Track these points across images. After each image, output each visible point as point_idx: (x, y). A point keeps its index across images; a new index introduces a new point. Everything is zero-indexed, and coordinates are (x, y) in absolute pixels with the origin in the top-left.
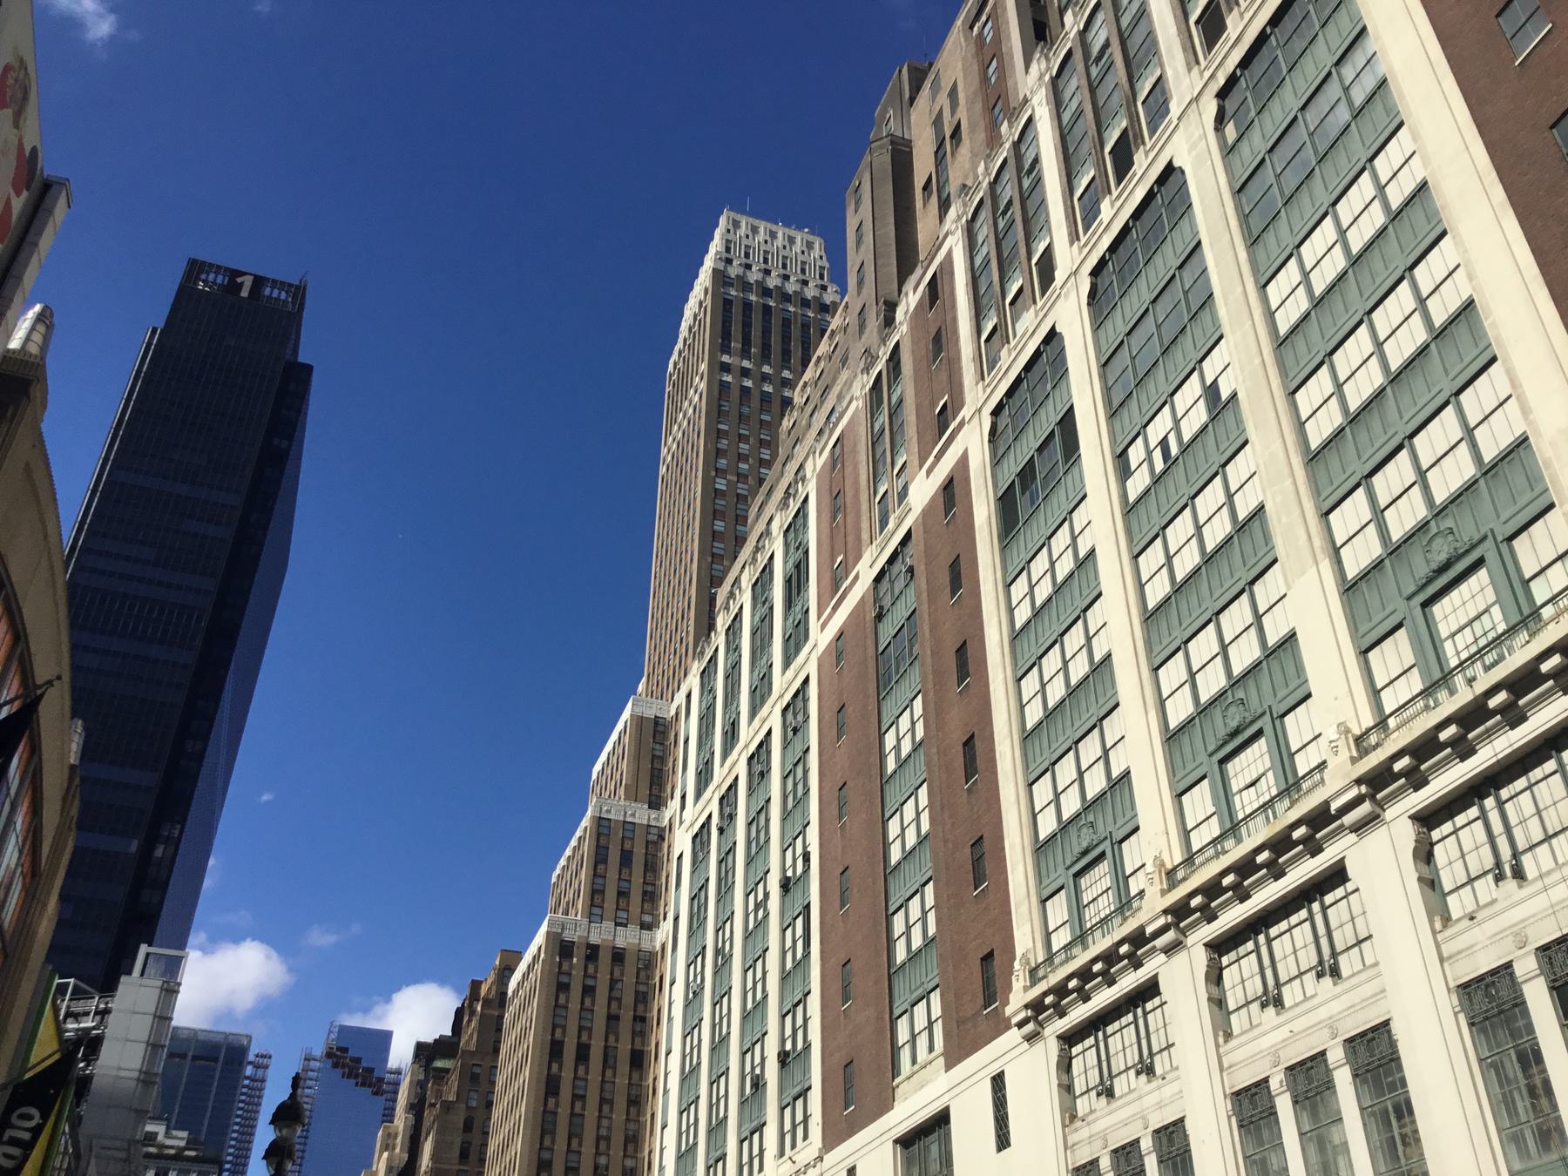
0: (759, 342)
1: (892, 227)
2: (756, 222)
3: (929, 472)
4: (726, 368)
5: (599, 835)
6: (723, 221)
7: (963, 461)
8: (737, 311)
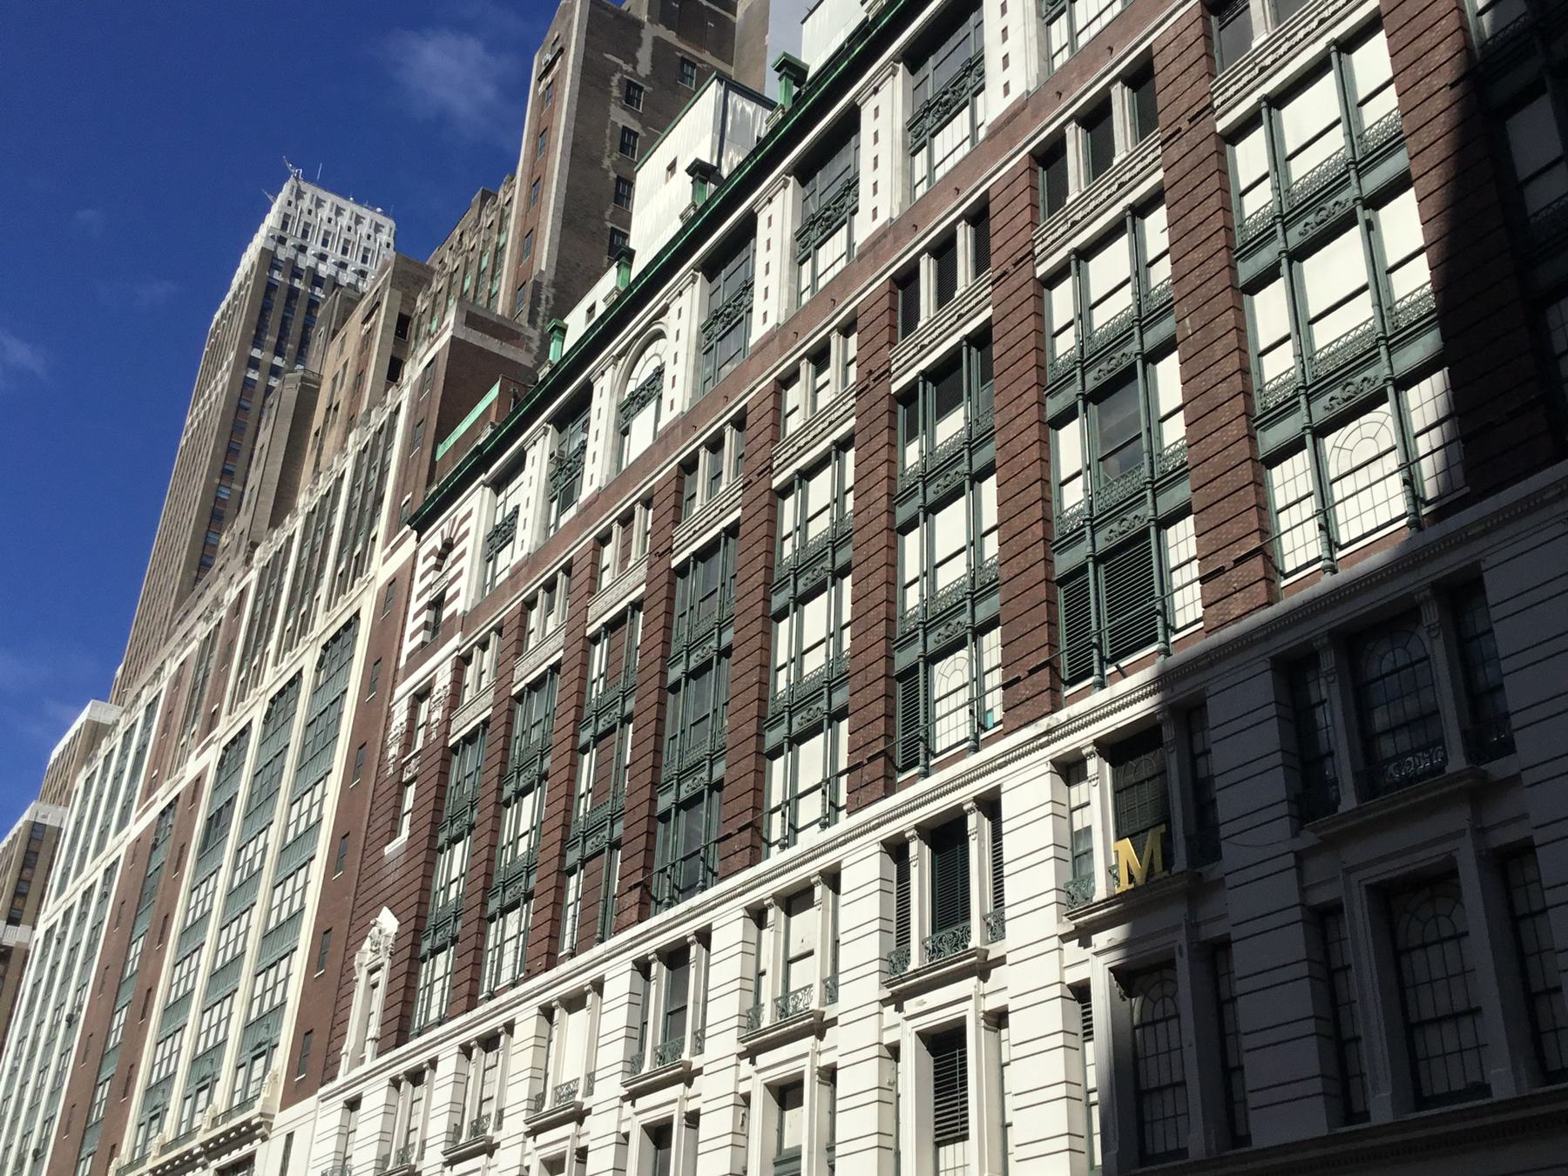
0: (297, 339)
1: (279, 467)
2: (322, 194)
3: (198, 756)
4: (254, 364)
5: (31, 838)
6: (286, 187)
7: (206, 769)
8: (279, 299)
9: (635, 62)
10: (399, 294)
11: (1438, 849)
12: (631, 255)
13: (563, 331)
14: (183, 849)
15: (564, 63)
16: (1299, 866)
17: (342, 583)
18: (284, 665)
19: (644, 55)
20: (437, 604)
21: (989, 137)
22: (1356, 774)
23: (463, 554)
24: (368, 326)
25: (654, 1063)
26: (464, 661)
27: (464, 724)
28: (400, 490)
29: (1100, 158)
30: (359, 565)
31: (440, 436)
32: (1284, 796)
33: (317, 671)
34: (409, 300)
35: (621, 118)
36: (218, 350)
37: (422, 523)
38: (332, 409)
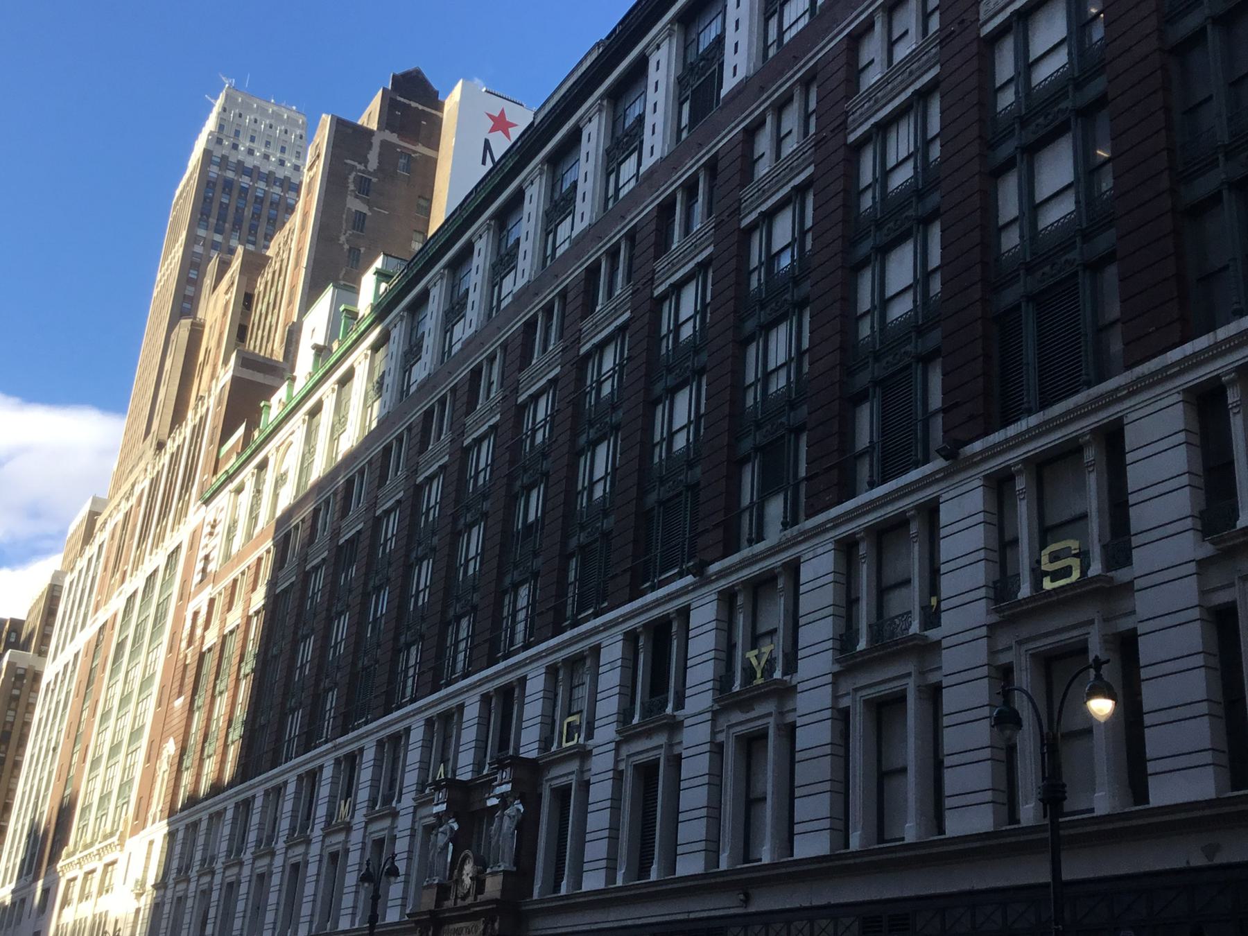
11: (1075, 633)
12: (293, 379)
13: (269, 407)
14: (106, 658)
16: (617, 750)
21: (418, 389)
30: (182, 513)
31: (223, 441)
32: (615, 710)
37: (207, 502)
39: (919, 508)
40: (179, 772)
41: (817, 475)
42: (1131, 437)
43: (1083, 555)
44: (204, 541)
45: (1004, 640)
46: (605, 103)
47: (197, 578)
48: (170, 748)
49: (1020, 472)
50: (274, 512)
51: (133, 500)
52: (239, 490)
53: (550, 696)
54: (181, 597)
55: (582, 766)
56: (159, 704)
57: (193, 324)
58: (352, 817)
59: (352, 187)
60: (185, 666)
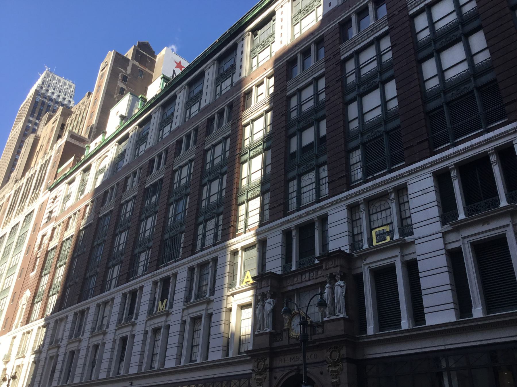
4: (30, 122)
6: (45, 73)
9: (126, 70)
10: (62, 118)
12: (105, 133)
13: (89, 147)
15: (107, 69)
17: (32, 200)
18: (30, 207)
19: (129, 69)
20: (51, 212)
22: (296, 262)
23: (58, 201)
24: (53, 125)
25: (125, 321)
26: (54, 229)
27: (53, 245)
28: (48, 179)
29: (220, 125)
30: (36, 197)
31: (60, 166)
33: (24, 222)
34: (65, 120)
35: (121, 85)
36: (20, 116)
37: (51, 190)
38: (42, 146)
39: (319, 217)
40: (33, 304)
41: (334, 181)
42: (330, 219)
43: (391, 233)
44: (48, 206)
45: (452, 237)
46: (216, 62)
47: (44, 221)
48: (28, 294)
49: (392, 192)
50: (95, 186)
51: (5, 200)
52: (70, 183)
53: (353, 221)
54: (34, 230)
55: (207, 307)
56: (20, 276)
57: (35, 136)
58: (171, 307)
59: (120, 78)
60: (37, 258)
